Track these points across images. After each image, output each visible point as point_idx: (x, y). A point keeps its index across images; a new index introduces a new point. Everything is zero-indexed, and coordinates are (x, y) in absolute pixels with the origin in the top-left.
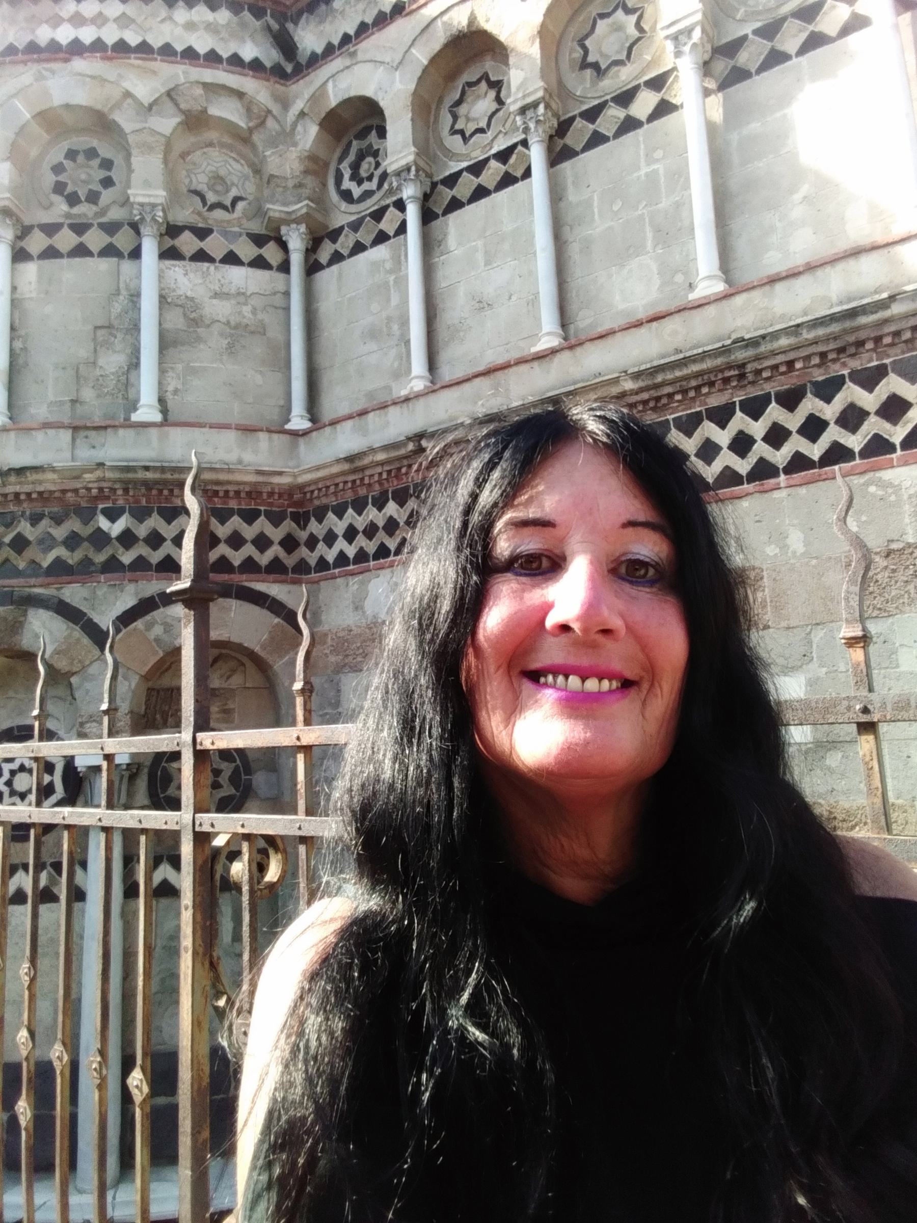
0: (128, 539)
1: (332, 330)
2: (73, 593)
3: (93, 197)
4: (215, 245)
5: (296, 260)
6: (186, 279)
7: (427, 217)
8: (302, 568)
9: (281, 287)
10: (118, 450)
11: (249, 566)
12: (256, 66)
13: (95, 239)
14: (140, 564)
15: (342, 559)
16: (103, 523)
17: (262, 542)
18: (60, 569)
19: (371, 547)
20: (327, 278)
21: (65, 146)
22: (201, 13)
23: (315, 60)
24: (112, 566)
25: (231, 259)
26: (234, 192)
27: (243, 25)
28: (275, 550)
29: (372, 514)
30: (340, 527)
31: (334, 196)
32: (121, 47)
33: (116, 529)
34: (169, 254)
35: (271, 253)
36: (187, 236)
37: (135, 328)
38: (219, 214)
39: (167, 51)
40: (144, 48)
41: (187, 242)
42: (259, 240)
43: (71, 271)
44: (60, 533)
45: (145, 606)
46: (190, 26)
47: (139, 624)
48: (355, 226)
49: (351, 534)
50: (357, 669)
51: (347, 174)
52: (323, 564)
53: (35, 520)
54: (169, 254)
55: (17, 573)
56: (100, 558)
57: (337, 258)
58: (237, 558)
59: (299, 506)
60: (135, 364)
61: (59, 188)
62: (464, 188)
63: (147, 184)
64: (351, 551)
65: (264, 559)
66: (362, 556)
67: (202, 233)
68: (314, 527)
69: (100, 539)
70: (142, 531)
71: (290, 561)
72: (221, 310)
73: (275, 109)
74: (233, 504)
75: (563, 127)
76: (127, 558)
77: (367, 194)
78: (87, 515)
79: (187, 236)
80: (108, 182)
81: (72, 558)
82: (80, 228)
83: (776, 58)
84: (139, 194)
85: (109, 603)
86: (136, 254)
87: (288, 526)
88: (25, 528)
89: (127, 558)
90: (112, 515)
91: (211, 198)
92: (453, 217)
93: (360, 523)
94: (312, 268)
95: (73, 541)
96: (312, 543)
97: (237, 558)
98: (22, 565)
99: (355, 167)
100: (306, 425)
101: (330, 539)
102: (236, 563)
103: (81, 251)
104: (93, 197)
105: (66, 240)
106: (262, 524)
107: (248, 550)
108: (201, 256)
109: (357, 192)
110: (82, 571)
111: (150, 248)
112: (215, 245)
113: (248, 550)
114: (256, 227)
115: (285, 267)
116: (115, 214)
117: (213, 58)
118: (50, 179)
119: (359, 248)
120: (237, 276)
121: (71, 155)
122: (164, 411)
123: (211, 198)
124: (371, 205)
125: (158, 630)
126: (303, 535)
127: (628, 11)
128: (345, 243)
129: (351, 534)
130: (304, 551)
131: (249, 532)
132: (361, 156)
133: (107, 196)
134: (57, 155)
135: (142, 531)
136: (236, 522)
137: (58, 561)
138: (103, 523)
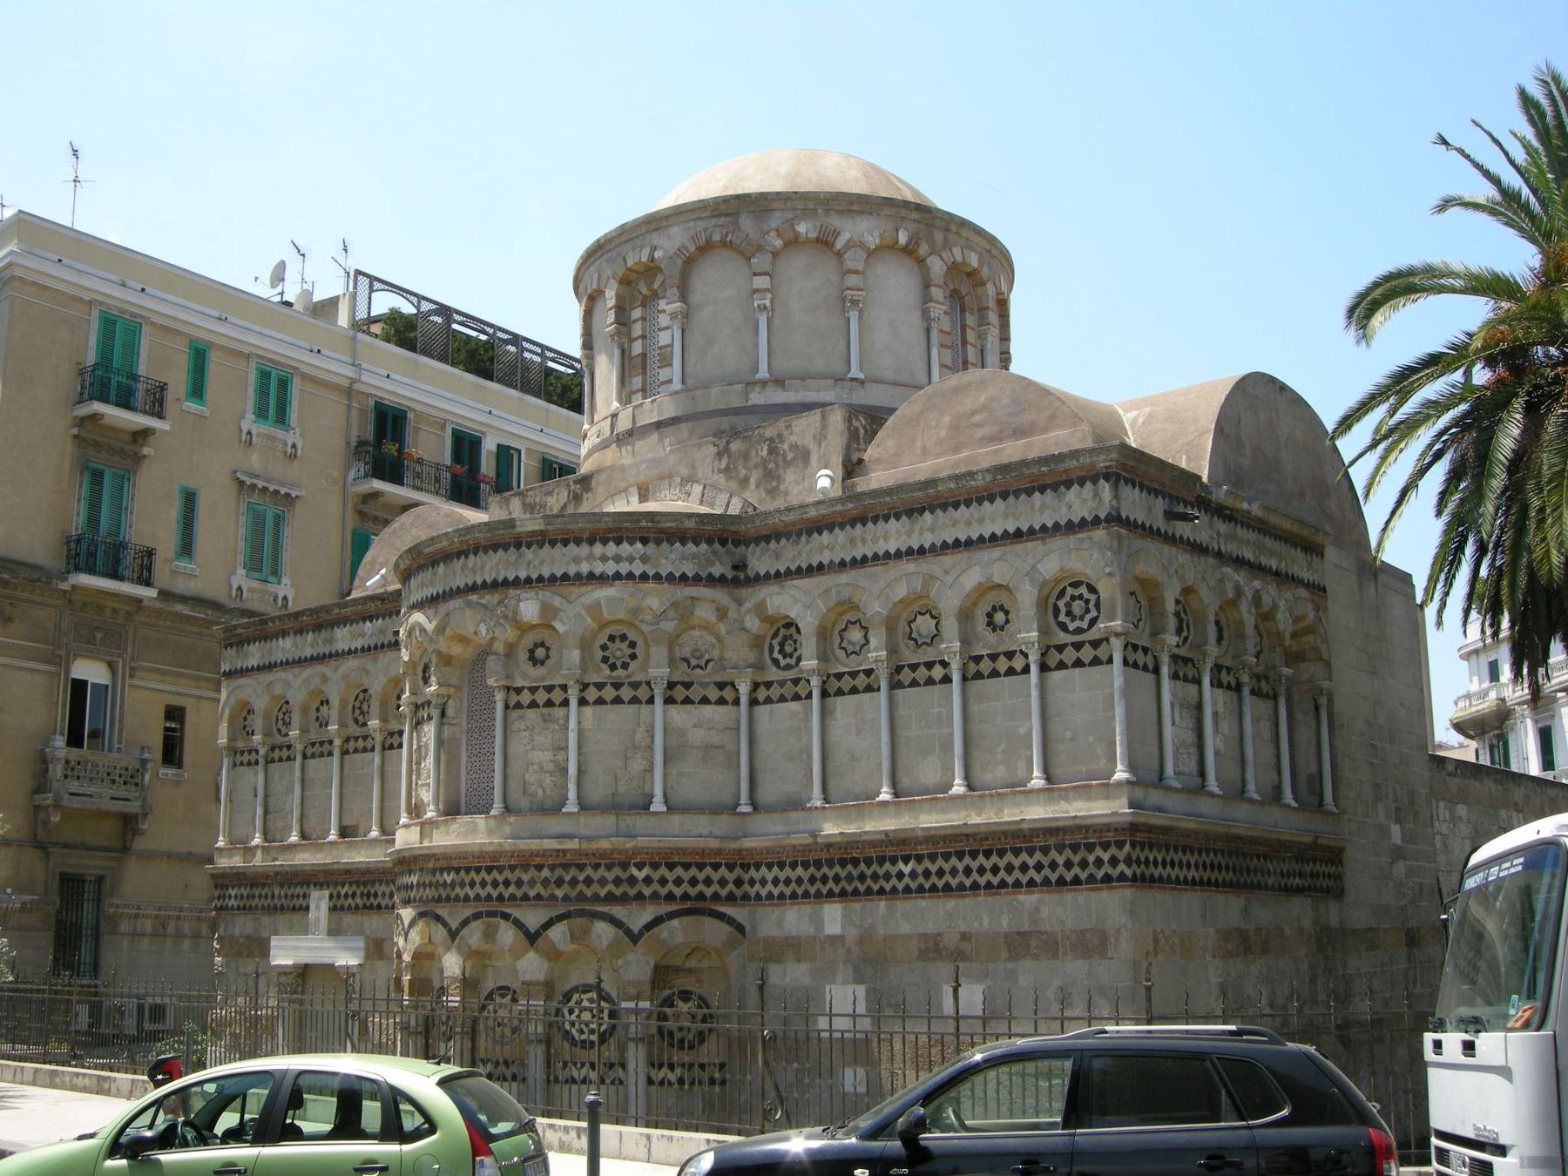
0: (648, 880)
1: (766, 747)
3: (625, 666)
4: (695, 693)
5: (744, 700)
6: (679, 715)
7: (824, 694)
8: (746, 897)
9: (734, 716)
11: (716, 897)
12: (722, 580)
13: (626, 693)
14: (655, 896)
15: (770, 896)
16: (635, 871)
17: (723, 882)
18: (610, 898)
19: (788, 892)
20: (763, 711)
21: (607, 632)
22: (691, 547)
23: (757, 579)
24: (640, 897)
25: (705, 701)
27: (715, 553)
28: (731, 887)
29: (788, 871)
30: (770, 876)
31: (769, 661)
32: (644, 577)
33: (641, 875)
34: (669, 701)
35: (728, 694)
37: (651, 748)
38: (698, 671)
39: (671, 578)
41: (679, 693)
42: (721, 686)
43: (613, 714)
44: (610, 876)
46: (683, 557)
47: (655, 930)
48: (782, 684)
49: (776, 882)
50: (779, 961)
51: (777, 649)
52: (758, 897)
53: (596, 867)
54: (669, 701)
56: (632, 892)
57: (768, 700)
58: (708, 892)
59: (745, 861)
60: (650, 770)
61: (605, 660)
62: (847, 683)
63: (659, 666)
64: (776, 892)
65: (724, 893)
66: (782, 896)
68: (753, 873)
69: (632, 881)
70: (656, 876)
71: (738, 893)
72: (697, 736)
73: (733, 606)
75: (899, 669)
76: (647, 892)
77: (788, 667)
78: (625, 866)
80: (633, 657)
81: (618, 892)
82: (617, 686)
83: (994, 674)
84: (654, 672)
85: (638, 917)
86: (651, 701)
87: (738, 871)
88: (589, 871)
89: (647, 892)
90: (640, 866)
91: (693, 662)
92: (839, 699)
93: (782, 876)
94: (753, 702)
95: (617, 881)
96: (752, 882)
97: (708, 892)
98: (589, 894)
99: (782, 645)
100: (748, 809)
101: (763, 882)
103: (618, 700)
104: (625, 666)
105: (609, 694)
106: (723, 871)
107: (715, 887)
108: (687, 701)
109: (783, 662)
110: (624, 899)
111: (659, 700)
112: (695, 693)
113: (715, 887)
114: (719, 679)
115: (737, 702)
116: (638, 677)
117: (697, 579)
118: (599, 654)
119: (782, 699)
120: (708, 710)
121: (612, 638)
122: (666, 802)
123: (693, 662)
124: (791, 674)
125: (665, 934)
126: (746, 877)
127: (933, 617)
128: (775, 692)
129: (776, 882)
130: (747, 887)
131: (715, 876)
132: (785, 638)
133: (633, 665)
134: (603, 638)
135: (656, 876)
136: (708, 870)
137: (610, 894)
138: (635, 871)
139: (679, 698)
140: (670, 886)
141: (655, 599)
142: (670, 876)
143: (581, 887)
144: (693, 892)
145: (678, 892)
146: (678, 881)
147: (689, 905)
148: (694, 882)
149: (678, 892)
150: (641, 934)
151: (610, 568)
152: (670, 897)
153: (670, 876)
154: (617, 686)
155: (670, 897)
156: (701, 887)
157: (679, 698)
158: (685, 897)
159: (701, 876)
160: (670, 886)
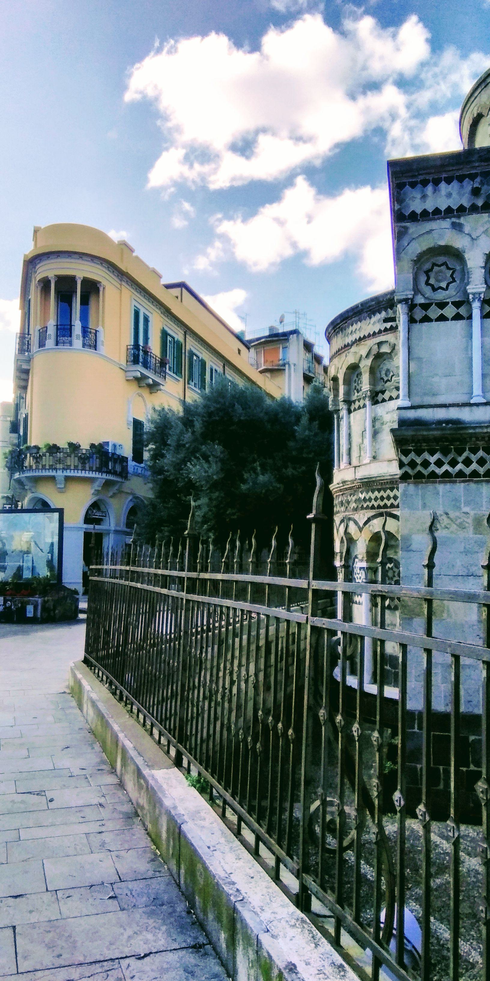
2: (356, 517)
10: (362, 473)
24: (362, 508)
26: (392, 374)
34: (375, 402)
36: (380, 395)
39: (369, 335)
40: (365, 337)
41: (380, 397)
44: (354, 499)
45: (369, 520)
47: (367, 526)
54: (375, 402)
55: (349, 511)
58: (389, 503)
63: (366, 384)
67: (383, 392)
74: (388, 486)
79: (380, 395)
91: (385, 379)
102: (389, 505)
107: (392, 501)
108: (384, 400)
112: (387, 396)
117: (380, 332)
123: (385, 379)
138: (360, 495)
139: (380, 400)
140: (373, 502)
141: (363, 350)
142: (373, 497)
143: (346, 505)
144: (382, 504)
145: (376, 504)
146: (376, 499)
147: (381, 510)
148: (382, 498)
149: (376, 504)
150: (363, 528)
151: (349, 340)
152: (373, 507)
153: (373, 497)
154: (359, 400)
155: (373, 507)
156: (386, 501)
157: (380, 400)
158: (379, 507)
159: (385, 495)
160: (373, 502)
